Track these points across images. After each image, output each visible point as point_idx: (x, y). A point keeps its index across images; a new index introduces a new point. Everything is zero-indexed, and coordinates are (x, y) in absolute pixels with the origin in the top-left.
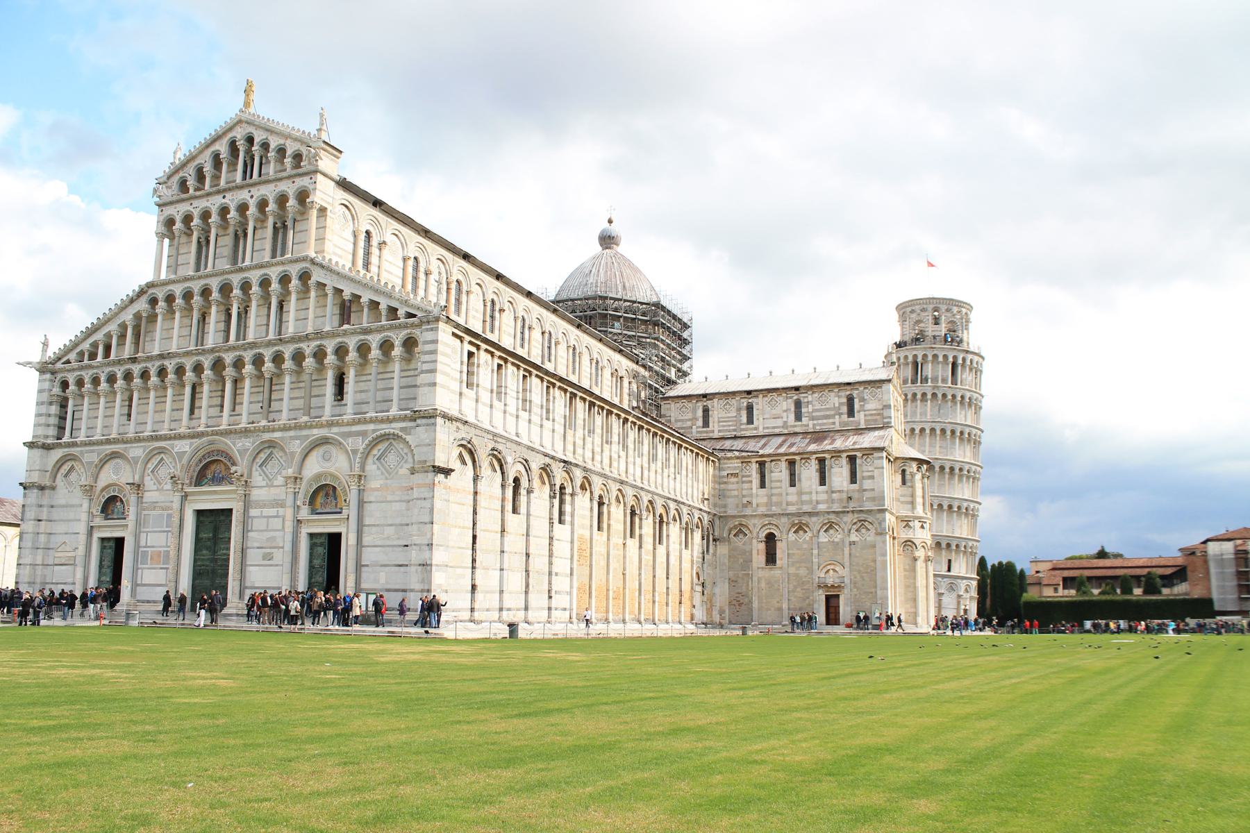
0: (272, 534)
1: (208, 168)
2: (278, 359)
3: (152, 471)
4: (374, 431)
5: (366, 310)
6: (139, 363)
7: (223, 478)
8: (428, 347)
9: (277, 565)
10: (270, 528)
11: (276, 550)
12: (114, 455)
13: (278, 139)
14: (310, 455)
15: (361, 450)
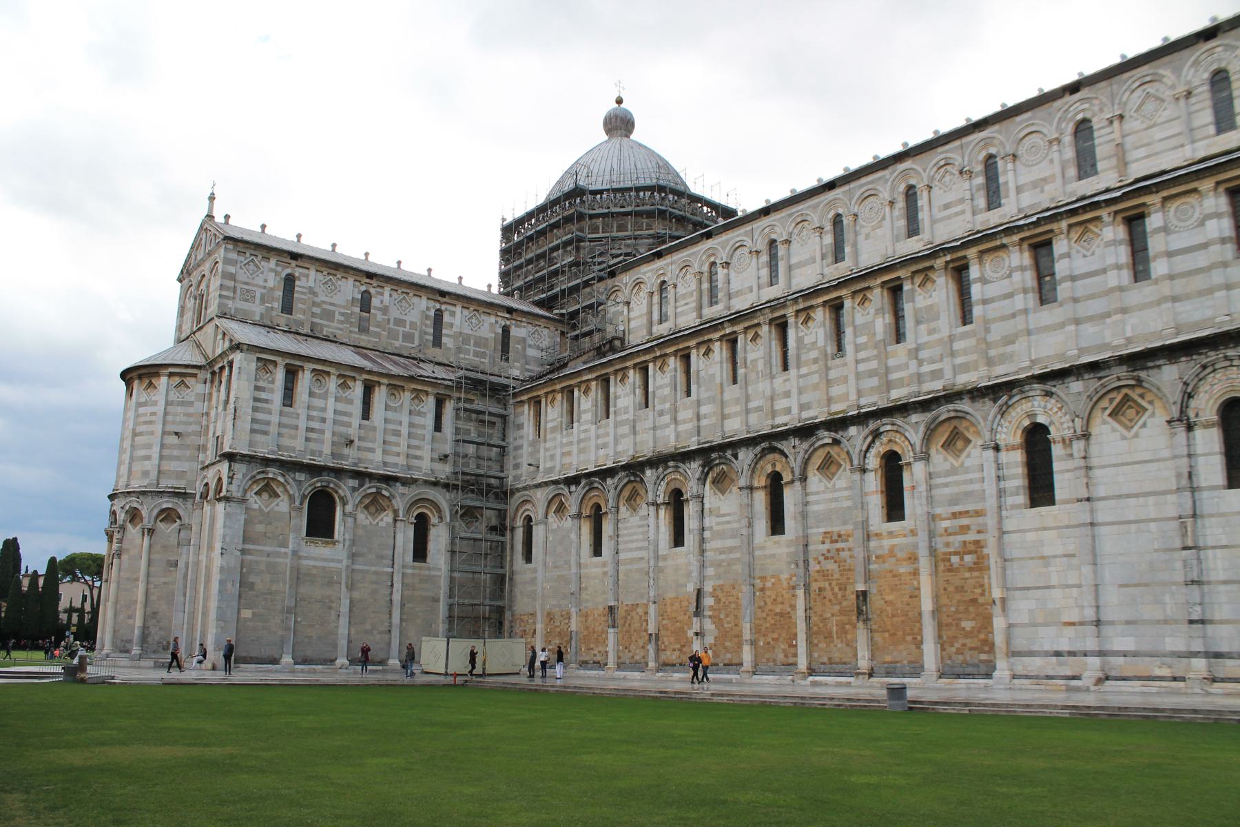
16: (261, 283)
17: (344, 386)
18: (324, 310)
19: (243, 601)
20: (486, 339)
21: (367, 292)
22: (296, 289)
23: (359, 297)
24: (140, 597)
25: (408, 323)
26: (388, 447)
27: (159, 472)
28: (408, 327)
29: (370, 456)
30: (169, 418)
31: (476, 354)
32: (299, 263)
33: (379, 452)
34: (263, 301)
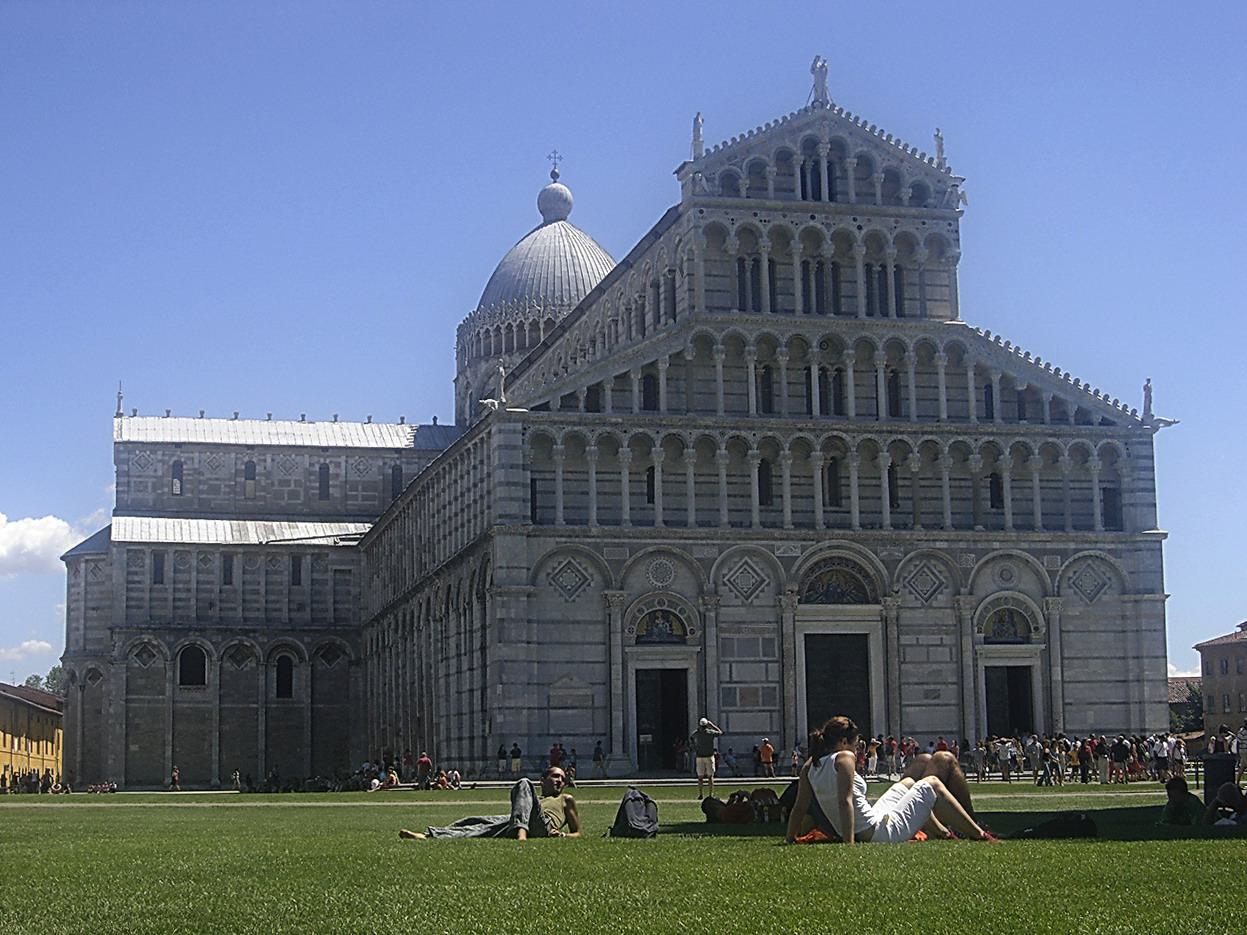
0: (935, 666)
1: (772, 169)
2: (931, 451)
3: (728, 580)
4: (1076, 551)
5: (1047, 407)
6: (695, 427)
7: (843, 594)
8: (1144, 463)
9: (946, 705)
10: (931, 660)
11: (944, 687)
12: (659, 552)
13: (887, 157)
14: (985, 570)
15: (1060, 573)
16: (152, 473)
17: (205, 561)
18: (211, 485)
19: (131, 738)
20: (375, 482)
21: (250, 461)
22: (185, 472)
23: (243, 467)
24: (79, 739)
25: (292, 482)
26: (248, 605)
27: (85, 639)
28: (293, 485)
29: (231, 614)
30: (89, 596)
31: (365, 498)
32: (184, 448)
33: (240, 609)
34: (154, 488)
